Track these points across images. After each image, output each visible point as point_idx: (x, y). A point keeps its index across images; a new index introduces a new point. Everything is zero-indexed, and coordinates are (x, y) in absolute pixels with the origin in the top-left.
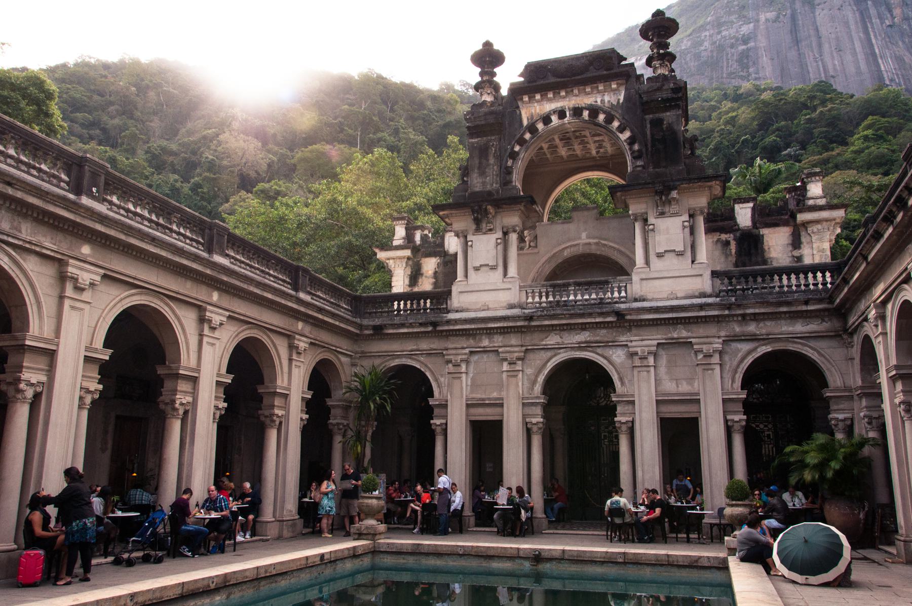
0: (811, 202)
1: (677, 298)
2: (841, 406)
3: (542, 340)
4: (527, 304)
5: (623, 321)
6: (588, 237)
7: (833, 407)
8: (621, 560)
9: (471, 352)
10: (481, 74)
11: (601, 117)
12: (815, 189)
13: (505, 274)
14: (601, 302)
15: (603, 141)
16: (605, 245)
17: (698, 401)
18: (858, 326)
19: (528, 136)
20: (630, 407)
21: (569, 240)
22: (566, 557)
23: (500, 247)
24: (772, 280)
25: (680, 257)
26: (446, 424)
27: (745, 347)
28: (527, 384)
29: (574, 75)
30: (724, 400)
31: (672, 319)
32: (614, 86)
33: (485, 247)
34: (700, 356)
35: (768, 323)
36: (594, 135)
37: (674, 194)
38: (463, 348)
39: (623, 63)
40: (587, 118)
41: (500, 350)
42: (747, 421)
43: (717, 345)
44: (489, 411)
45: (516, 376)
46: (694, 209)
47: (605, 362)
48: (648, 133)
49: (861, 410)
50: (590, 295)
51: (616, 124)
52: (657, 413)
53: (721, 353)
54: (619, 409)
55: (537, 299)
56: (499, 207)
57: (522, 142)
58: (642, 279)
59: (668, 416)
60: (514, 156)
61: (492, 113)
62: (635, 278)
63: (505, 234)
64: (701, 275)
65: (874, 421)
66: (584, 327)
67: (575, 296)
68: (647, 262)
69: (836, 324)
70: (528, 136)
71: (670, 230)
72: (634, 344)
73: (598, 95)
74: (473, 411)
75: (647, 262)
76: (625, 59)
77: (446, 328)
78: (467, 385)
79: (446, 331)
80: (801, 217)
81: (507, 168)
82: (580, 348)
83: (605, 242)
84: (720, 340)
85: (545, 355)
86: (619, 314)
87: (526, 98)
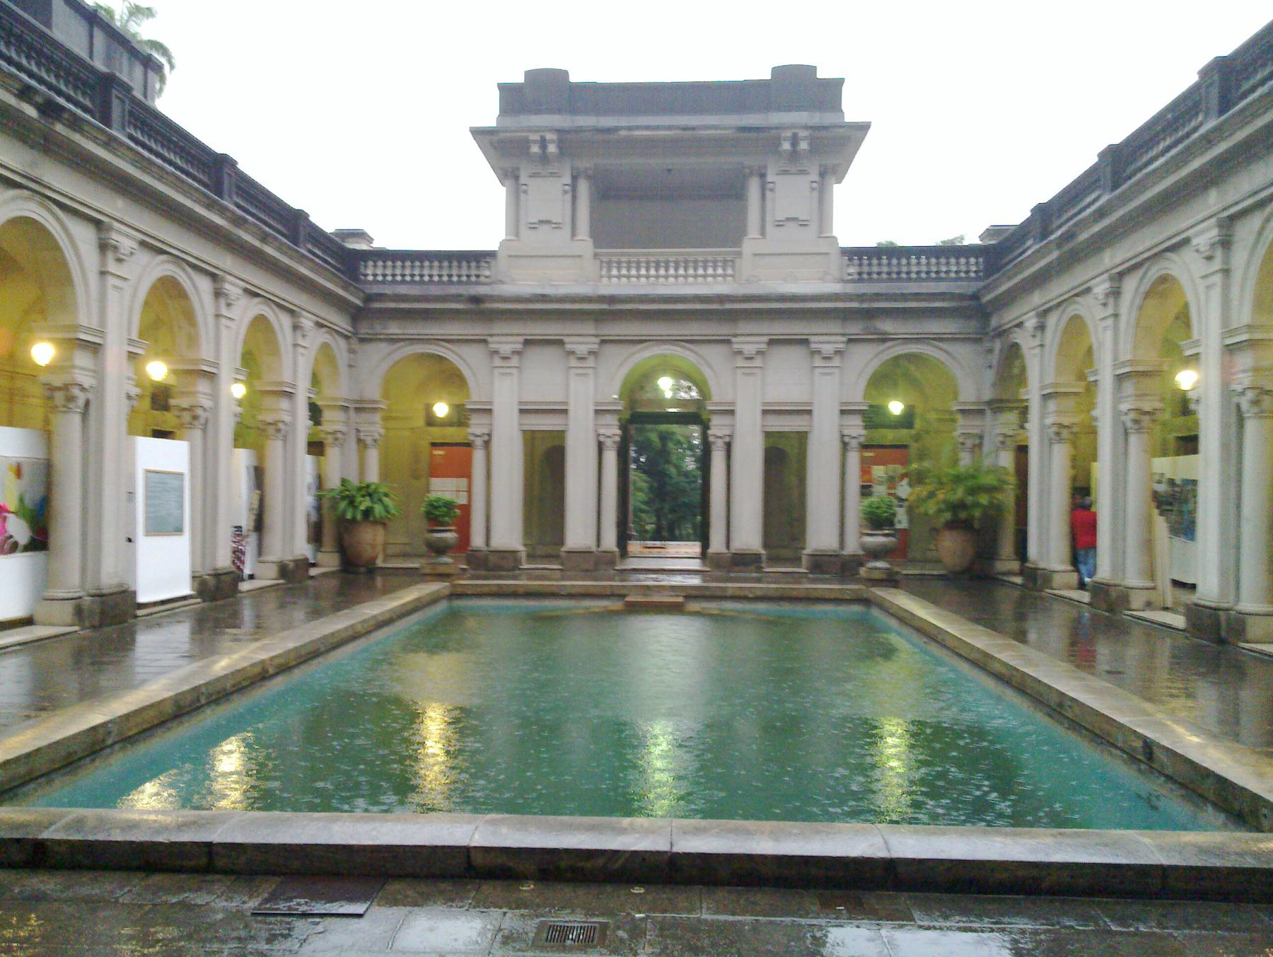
13: (573, 234)
23: (569, 197)
26: (489, 435)
54: (716, 421)
58: (755, 255)
63: (575, 178)
68: (763, 233)
69: (973, 325)
75: (763, 233)
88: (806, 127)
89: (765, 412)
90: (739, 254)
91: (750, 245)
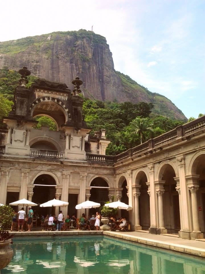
0: (102, 138)
1: (77, 160)
2: (112, 193)
3: (36, 167)
4: (32, 155)
5: (62, 165)
6: (46, 136)
7: (110, 192)
8: (77, 234)
9: (11, 169)
10: (22, 77)
11: (60, 103)
12: (103, 134)
13: (25, 144)
14: (55, 158)
15: (53, 107)
16: (51, 139)
17: (79, 189)
18: (120, 174)
19: (37, 102)
20: (61, 190)
21: (40, 136)
22: (62, 234)
24: (92, 158)
25: (79, 148)
27: (92, 175)
28: (29, 181)
29: (54, 88)
30: (86, 190)
31: (76, 166)
32: (65, 95)
33: (19, 134)
34: (81, 177)
35: (98, 170)
36: (51, 105)
37: (79, 131)
38: (8, 167)
39: (67, 89)
40: (56, 102)
41: (22, 169)
42: (91, 196)
43: (85, 174)
44: (15, 188)
45: (26, 178)
46: (83, 136)
47: (55, 176)
48: (73, 111)
49: (116, 194)
50: (52, 155)
51: (64, 106)
52: (69, 192)
53: (86, 177)
54: (57, 190)
55: (35, 154)
56: (26, 123)
57: (35, 103)
58: (68, 153)
59: (71, 193)
60: (32, 106)
61: (26, 91)
62: (66, 152)
64: (83, 154)
65: (120, 197)
66: (50, 165)
67: (47, 155)
68: (69, 148)
70: (37, 102)
71: (76, 140)
72: (64, 171)
73: (60, 96)
74: (9, 188)
75: (69, 148)
76: (68, 88)
77: (3, 159)
78: (8, 180)
79: (3, 160)
80: (101, 141)
81: (29, 110)
82: (48, 171)
83: (51, 138)
84: (87, 173)
85: (36, 172)
86: (62, 163)
87: (38, 90)
90: (65, 152)
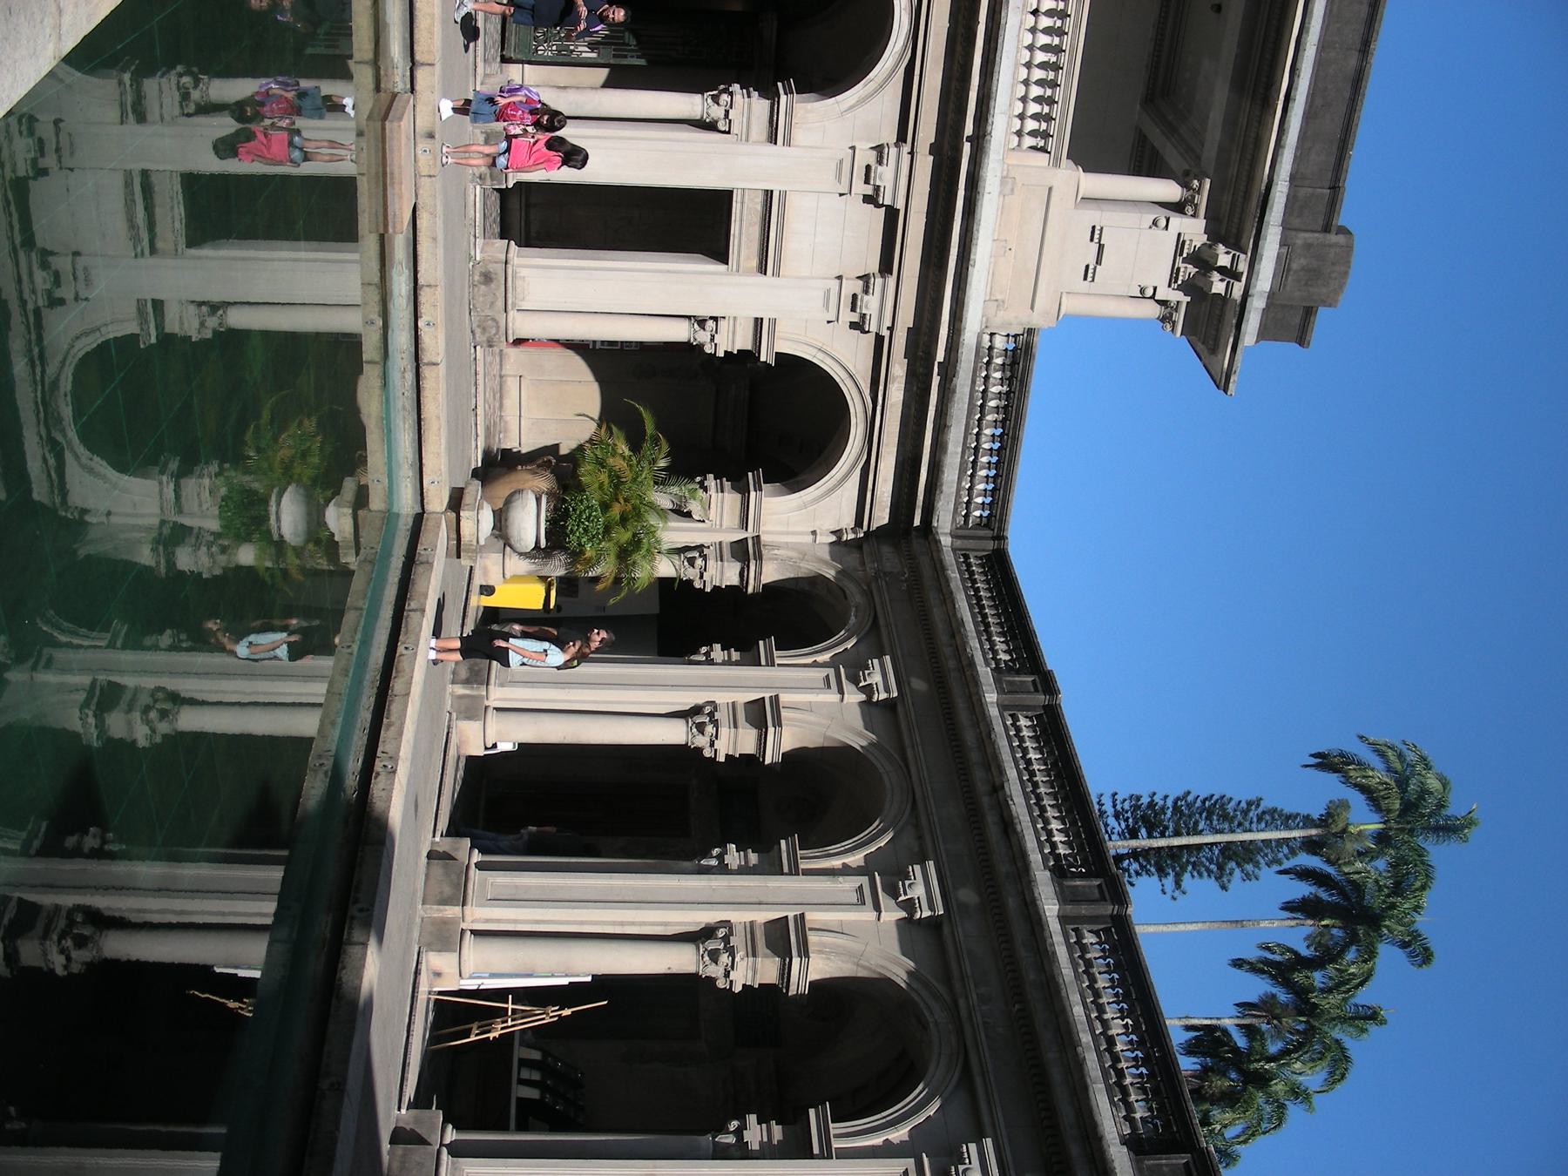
54: (760, 106)
88: (1246, 295)
89: (768, 194)
90: (1057, 163)
91: (1072, 180)
